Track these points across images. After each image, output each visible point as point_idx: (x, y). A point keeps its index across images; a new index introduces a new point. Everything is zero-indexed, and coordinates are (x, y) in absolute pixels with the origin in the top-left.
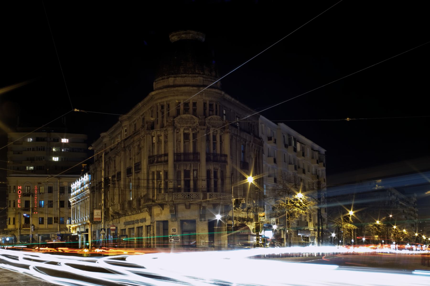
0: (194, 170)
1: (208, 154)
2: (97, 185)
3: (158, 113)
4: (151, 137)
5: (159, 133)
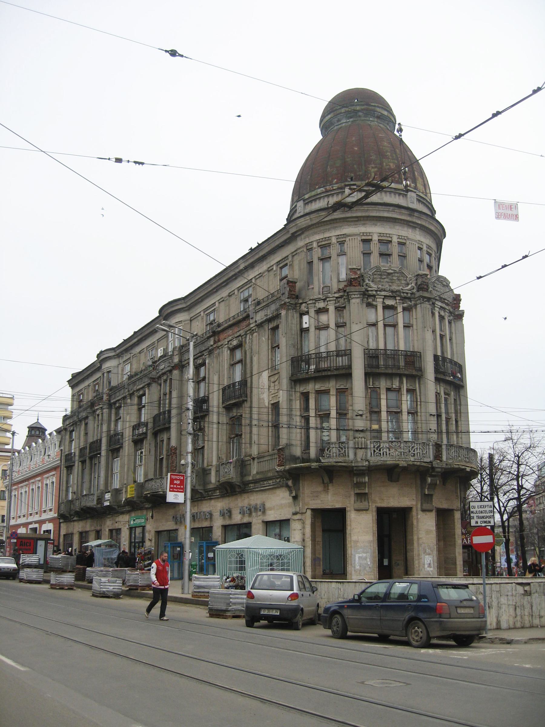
0: (408, 391)
1: (436, 357)
2: (82, 450)
3: (310, 263)
5: (321, 305)
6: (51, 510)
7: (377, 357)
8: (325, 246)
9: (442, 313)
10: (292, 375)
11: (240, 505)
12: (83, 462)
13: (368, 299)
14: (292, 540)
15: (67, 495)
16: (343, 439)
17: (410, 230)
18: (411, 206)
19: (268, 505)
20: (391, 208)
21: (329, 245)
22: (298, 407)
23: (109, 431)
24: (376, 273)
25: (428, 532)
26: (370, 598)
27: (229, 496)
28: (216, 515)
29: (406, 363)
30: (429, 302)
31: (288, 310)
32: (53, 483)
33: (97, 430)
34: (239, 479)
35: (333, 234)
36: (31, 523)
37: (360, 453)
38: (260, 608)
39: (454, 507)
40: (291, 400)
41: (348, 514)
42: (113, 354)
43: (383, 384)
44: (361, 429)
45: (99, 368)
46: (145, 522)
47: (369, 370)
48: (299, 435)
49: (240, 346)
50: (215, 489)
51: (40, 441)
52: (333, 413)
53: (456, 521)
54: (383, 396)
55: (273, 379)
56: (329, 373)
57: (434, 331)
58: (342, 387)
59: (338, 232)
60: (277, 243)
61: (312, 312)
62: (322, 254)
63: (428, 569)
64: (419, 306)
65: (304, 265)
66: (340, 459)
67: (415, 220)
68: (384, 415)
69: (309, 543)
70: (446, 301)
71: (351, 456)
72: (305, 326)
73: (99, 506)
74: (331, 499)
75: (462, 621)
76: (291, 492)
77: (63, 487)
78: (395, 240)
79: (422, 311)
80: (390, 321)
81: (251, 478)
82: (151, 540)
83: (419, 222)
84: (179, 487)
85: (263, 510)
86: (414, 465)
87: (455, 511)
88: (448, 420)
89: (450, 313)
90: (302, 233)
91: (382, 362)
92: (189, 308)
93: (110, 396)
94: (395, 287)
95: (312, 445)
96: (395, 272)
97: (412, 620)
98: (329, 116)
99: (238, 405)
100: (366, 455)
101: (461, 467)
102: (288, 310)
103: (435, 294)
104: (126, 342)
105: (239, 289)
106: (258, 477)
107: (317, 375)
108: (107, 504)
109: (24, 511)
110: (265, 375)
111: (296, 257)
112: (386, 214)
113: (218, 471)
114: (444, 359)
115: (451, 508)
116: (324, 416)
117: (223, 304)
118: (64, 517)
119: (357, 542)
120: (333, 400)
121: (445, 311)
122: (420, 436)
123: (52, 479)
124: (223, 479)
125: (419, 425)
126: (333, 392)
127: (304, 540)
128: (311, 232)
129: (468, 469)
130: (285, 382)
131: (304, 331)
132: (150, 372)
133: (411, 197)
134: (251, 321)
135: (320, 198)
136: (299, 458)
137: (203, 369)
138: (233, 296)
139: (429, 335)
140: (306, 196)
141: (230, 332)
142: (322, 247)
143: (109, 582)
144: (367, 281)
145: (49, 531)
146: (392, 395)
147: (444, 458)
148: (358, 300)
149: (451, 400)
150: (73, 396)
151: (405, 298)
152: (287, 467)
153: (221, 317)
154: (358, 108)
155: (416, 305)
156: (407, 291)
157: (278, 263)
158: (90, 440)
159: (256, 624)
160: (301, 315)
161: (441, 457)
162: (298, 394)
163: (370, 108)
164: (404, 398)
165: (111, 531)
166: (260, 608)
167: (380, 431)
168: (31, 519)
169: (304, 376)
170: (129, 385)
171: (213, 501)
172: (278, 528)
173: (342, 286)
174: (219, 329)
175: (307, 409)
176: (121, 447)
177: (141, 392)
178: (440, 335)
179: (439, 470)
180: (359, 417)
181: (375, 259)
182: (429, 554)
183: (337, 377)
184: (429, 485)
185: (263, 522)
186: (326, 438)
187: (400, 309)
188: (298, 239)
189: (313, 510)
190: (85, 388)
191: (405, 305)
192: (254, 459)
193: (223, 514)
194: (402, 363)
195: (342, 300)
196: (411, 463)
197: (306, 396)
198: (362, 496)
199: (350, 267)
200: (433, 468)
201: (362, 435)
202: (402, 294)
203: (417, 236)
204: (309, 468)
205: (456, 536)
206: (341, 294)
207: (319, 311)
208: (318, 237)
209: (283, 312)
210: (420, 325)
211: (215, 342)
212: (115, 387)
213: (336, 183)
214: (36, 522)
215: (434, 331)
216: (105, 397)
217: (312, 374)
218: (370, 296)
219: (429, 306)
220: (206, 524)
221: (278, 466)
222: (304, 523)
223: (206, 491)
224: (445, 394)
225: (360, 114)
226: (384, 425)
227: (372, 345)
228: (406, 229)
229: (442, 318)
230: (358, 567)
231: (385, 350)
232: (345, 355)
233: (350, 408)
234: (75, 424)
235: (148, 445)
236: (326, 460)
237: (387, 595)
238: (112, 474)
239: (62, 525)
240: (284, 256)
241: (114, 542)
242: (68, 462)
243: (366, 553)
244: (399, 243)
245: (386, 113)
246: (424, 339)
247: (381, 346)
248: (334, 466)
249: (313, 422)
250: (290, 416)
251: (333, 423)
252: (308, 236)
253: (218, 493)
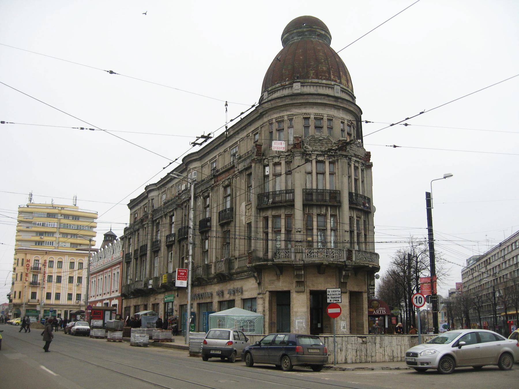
1: (350, 194)
2: (136, 251)
3: (271, 133)
4: (261, 167)
5: (277, 160)
6: (117, 291)
7: (311, 194)
8: (280, 121)
9: (357, 165)
10: (258, 205)
11: (228, 288)
12: (136, 259)
13: (306, 156)
14: (257, 311)
15: (127, 281)
16: (289, 246)
17: (336, 111)
18: (336, 95)
19: (244, 289)
21: (283, 121)
22: (261, 226)
23: (152, 239)
26: (266, 344)
27: (222, 282)
28: (215, 294)
29: (331, 198)
31: (256, 163)
32: (118, 273)
33: (145, 238)
34: (227, 272)
35: (285, 114)
36: (105, 300)
37: (299, 256)
38: (210, 350)
39: (363, 291)
40: (257, 221)
41: (291, 294)
42: (156, 187)
43: (315, 211)
44: (299, 240)
45: (147, 197)
46: (173, 299)
47: (306, 202)
48: (262, 244)
49: (229, 185)
50: (214, 278)
51: (110, 244)
52: (283, 230)
53: (364, 299)
54: (315, 219)
55: (248, 207)
56: (281, 204)
57: (350, 177)
58: (289, 213)
59: (289, 113)
60: (252, 118)
61: (271, 164)
62: (279, 126)
63: (343, 330)
64: (339, 160)
65: (267, 134)
66: (286, 260)
67: (338, 104)
68: (315, 231)
69: (267, 313)
71: (293, 258)
72: (267, 174)
73: (145, 288)
74: (281, 285)
75: (314, 356)
76: (257, 281)
77: (124, 276)
78: (325, 118)
79: (341, 164)
80: (321, 171)
81: (234, 271)
82: (177, 311)
84: (184, 277)
85: (241, 291)
86: (333, 263)
87: (364, 293)
88: (359, 235)
89: (363, 164)
90: (267, 113)
91: (314, 197)
92: (201, 159)
93: (153, 215)
95: (270, 250)
97: (284, 356)
98: (286, 35)
99: (228, 223)
100: (302, 257)
102: (256, 163)
103: (351, 153)
104: (162, 180)
105: (230, 147)
106: (238, 270)
107: (273, 205)
108: (150, 287)
109: (100, 292)
110: (244, 204)
111: (263, 128)
112: (319, 101)
113: (215, 266)
114: (357, 194)
115: (360, 291)
116: (278, 232)
117: (221, 156)
118: (124, 296)
119: (296, 312)
120: (283, 222)
121: (358, 163)
122: (339, 245)
123: (117, 270)
124: (218, 272)
125: (339, 238)
126: (283, 217)
127: (264, 311)
128: (271, 112)
129: (371, 266)
130: (253, 209)
131: (266, 177)
132: (177, 200)
133: (337, 89)
134: (236, 169)
135: (278, 91)
136: (261, 259)
137: (208, 199)
138: (227, 152)
139: (346, 180)
140: (270, 89)
141: (224, 176)
142: (279, 122)
143: (140, 337)
144: (306, 145)
145: (115, 305)
146: (321, 219)
147: (354, 259)
148: (299, 158)
149: (362, 222)
150: (131, 214)
151: (331, 155)
152: (254, 264)
153: (219, 166)
154: (305, 30)
155: (338, 160)
157: (253, 132)
158: (141, 244)
159: (209, 359)
160: (265, 166)
162: (262, 218)
163: (313, 29)
164: (328, 221)
165: (153, 305)
166: (210, 350)
167: (312, 242)
168: (105, 297)
169: (265, 206)
170: (164, 208)
171: (213, 285)
172: (249, 303)
173: (290, 148)
174: (217, 174)
175: (267, 227)
176: (159, 250)
177: (172, 214)
178: (355, 179)
180: (298, 233)
181: (312, 130)
182: (344, 320)
183: (285, 207)
184: (344, 276)
185: (241, 299)
186: (278, 246)
187: (327, 163)
188: (264, 116)
189: (270, 292)
190: (138, 210)
192: (236, 259)
193: (218, 294)
194: (328, 198)
195: (289, 157)
196: (331, 262)
197: (266, 219)
198: (300, 283)
199: (295, 136)
200: (346, 266)
201: (300, 244)
203: (341, 114)
204: (267, 265)
205: (364, 309)
206: (289, 153)
207: (276, 164)
208: (276, 116)
209: (253, 165)
210: (340, 173)
211: (215, 182)
212: (157, 209)
213: (288, 81)
214: (108, 299)
215: (350, 177)
216: (150, 216)
217: (271, 204)
218: (307, 154)
219: (346, 161)
220: (209, 300)
221: (249, 263)
222: (264, 300)
223: (209, 279)
224: (357, 217)
225: (306, 33)
226: (315, 238)
227: (309, 186)
228: (333, 110)
229: (356, 168)
230: (297, 328)
231: (317, 189)
232: (291, 193)
233: (293, 227)
234: (131, 234)
235: (175, 248)
236: (277, 260)
237: (273, 342)
238: (154, 267)
239: (124, 301)
240: (256, 127)
241: (154, 312)
242: (127, 259)
243: (303, 319)
244: (328, 120)
245: (323, 32)
246: (342, 182)
247: (314, 187)
248: (282, 264)
249: (270, 236)
250: (257, 232)
251: (283, 236)
252: (270, 115)
253: (216, 280)
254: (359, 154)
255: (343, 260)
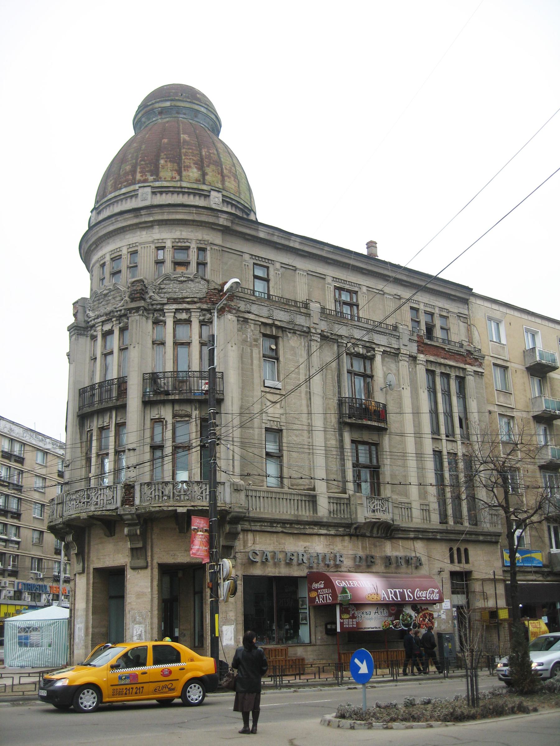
17: (144, 233)
20: (113, 219)
24: (95, 299)
25: (139, 595)
30: (137, 312)
70: (188, 300)
83: (151, 219)
94: (109, 308)
96: (110, 291)
101: (165, 509)
112: (111, 228)
129: (180, 510)
147: (137, 501)
156: (120, 308)
161: (134, 500)
179: (129, 517)
182: (140, 623)
191: (121, 325)
196: (91, 514)
202: (116, 314)
245: (168, 104)
254: (185, 295)
255: (113, 507)
